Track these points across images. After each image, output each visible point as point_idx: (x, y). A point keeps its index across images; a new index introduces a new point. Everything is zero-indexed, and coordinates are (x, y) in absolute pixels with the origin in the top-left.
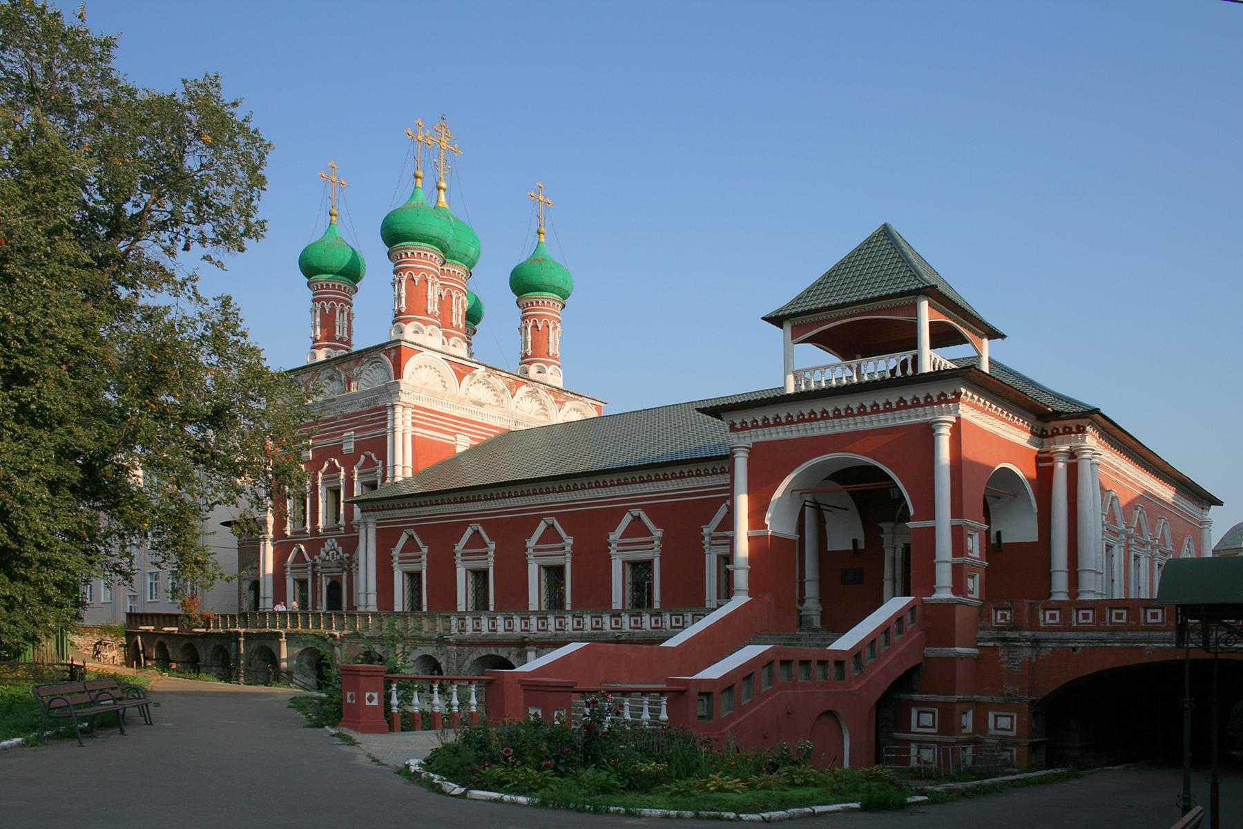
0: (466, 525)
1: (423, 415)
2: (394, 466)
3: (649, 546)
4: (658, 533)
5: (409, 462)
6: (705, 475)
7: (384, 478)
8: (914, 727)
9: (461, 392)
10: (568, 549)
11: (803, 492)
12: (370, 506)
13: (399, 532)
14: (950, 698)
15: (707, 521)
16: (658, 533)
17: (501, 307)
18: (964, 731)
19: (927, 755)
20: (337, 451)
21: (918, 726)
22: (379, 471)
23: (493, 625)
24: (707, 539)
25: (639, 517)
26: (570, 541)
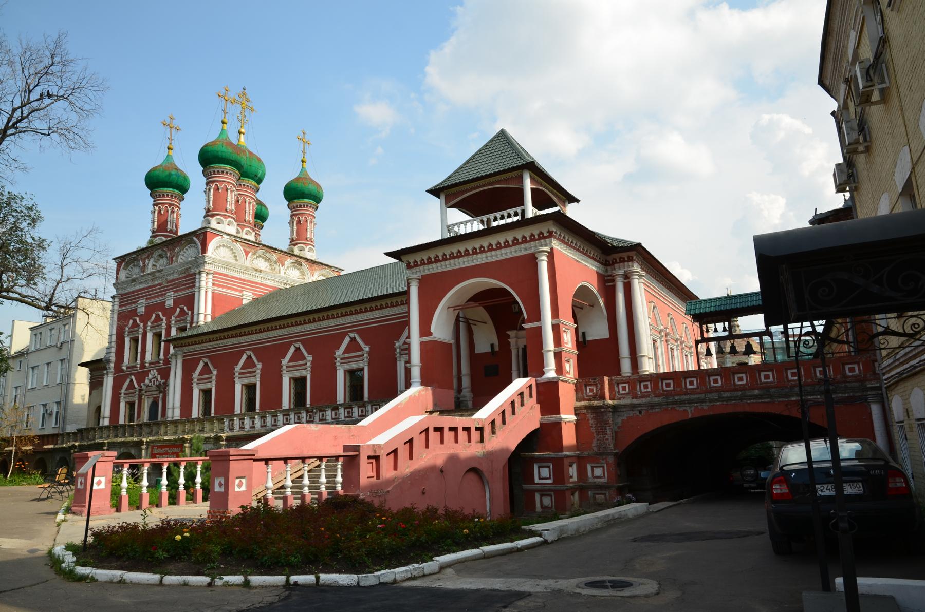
0: (243, 352)
2: (199, 314)
4: (367, 349)
5: (209, 311)
7: (192, 323)
8: (537, 480)
9: (247, 263)
10: (309, 364)
11: (455, 308)
12: (179, 343)
13: (197, 361)
14: (560, 455)
16: (367, 349)
17: (279, 209)
18: (571, 480)
19: (547, 501)
20: (161, 306)
21: (540, 478)
22: (189, 319)
23: (275, 421)
24: (398, 350)
26: (310, 358)
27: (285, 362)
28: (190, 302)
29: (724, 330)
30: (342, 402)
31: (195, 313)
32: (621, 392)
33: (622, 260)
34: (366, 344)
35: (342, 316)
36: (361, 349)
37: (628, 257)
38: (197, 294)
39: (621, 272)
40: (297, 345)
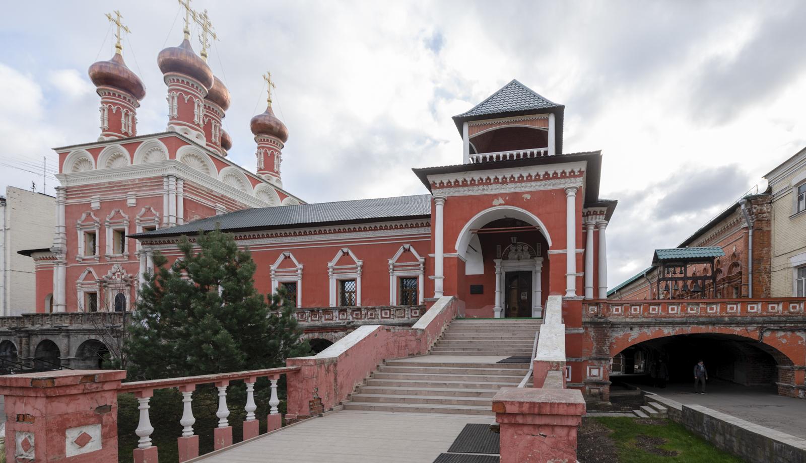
1: (187, 187)
3: (354, 270)
4: (360, 263)
6: (390, 229)
10: (300, 271)
15: (392, 255)
25: (348, 253)
26: (301, 266)
27: (273, 267)
28: (158, 202)
29: (681, 273)
30: (335, 306)
31: (165, 214)
32: (614, 312)
33: (595, 213)
34: (359, 258)
35: (335, 232)
36: (354, 263)
37: (601, 212)
38: (165, 197)
39: (594, 222)
40: (287, 254)
